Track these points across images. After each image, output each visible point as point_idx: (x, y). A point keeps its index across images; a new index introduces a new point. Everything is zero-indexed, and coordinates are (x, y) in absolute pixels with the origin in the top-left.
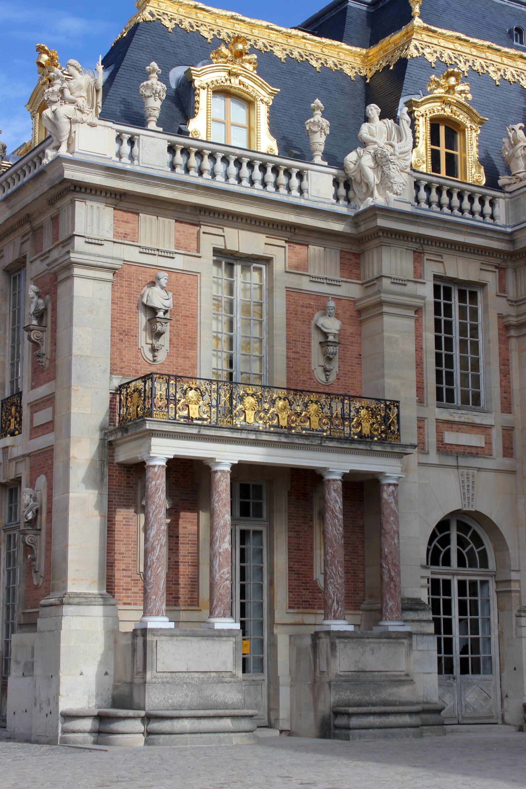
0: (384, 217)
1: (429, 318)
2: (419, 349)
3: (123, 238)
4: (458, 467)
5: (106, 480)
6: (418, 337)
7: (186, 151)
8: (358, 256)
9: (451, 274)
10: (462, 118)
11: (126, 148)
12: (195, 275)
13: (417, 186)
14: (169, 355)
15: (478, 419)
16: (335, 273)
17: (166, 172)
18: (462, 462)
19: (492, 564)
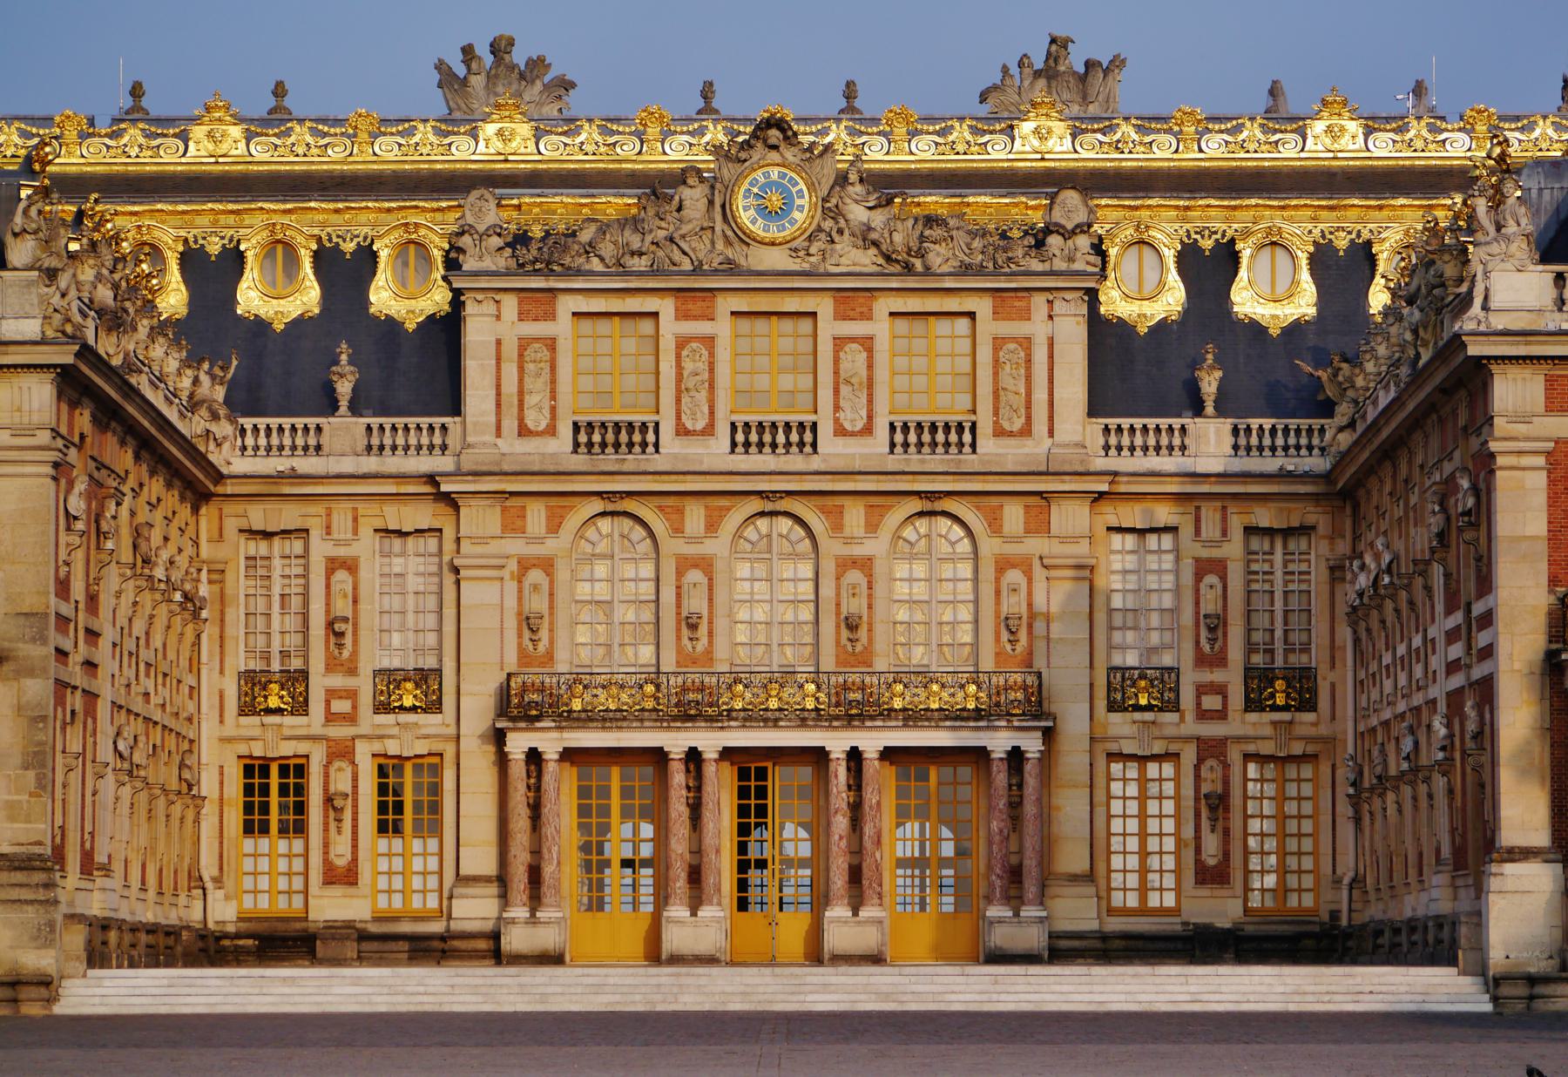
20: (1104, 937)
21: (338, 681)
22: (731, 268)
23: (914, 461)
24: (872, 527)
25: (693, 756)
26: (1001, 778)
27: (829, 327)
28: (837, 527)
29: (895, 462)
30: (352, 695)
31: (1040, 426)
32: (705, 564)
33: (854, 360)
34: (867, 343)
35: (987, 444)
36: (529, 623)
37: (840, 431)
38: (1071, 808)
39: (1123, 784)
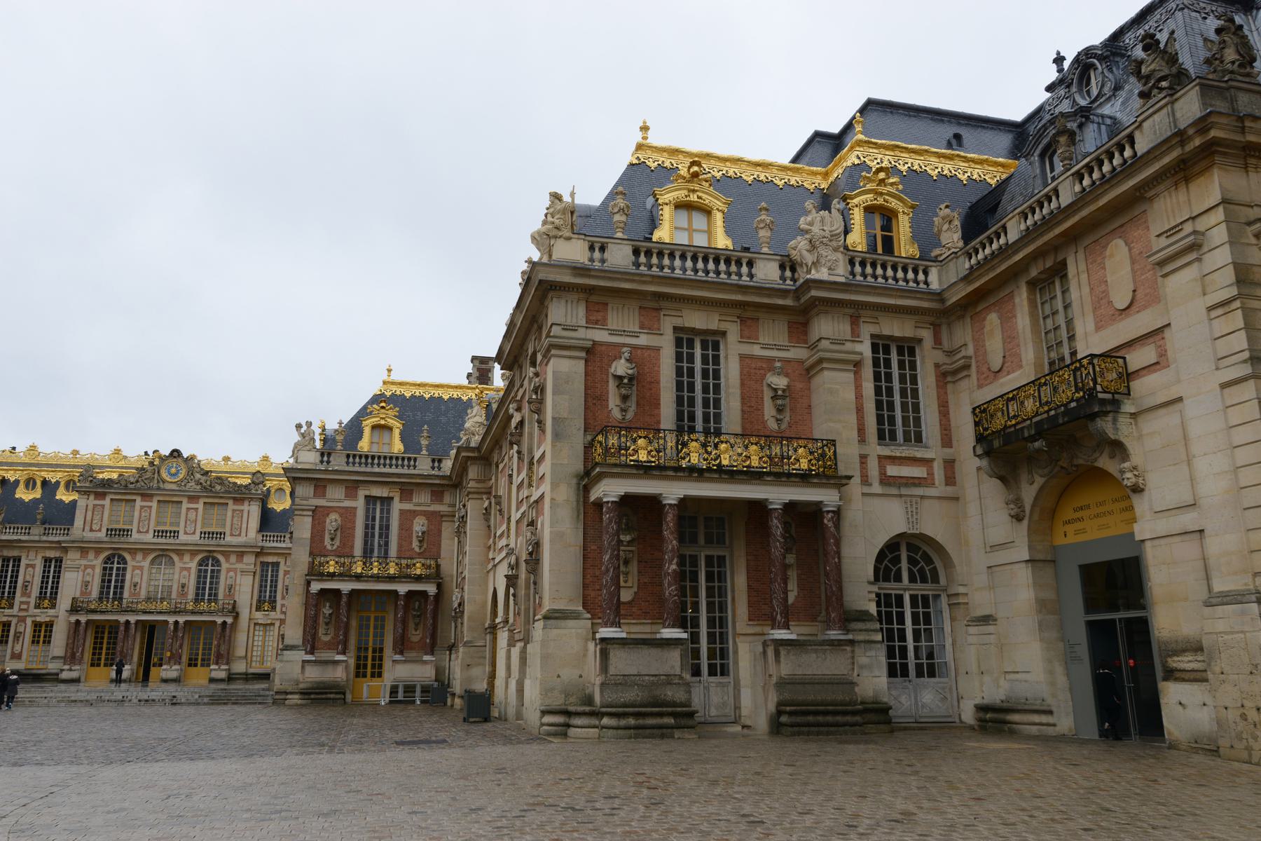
0: (818, 288)
1: (868, 372)
2: (859, 396)
3: (592, 323)
4: (901, 496)
5: (582, 517)
6: (858, 387)
7: (649, 253)
8: (806, 324)
9: (886, 332)
10: (894, 204)
11: (597, 254)
12: (657, 349)
13: (852, 262)
14: (636, 414)
15: (919, 453)
16: (783, 339)
17: (632, 269)
18: (904, 491)
19: (943, 581)
20: (246, 674)
21: (24, 599)
22: (159, 488)
23: (206, 542)
24: (192, 559)
25: (128, 622)
26: (219, 629)
27: (185, 505)
28: (181, 559)
29: (202, 542)
30: (28, 603)
31: (243, 534)
32: (141, 568)
33: (192, 515)
34: (196, 509)
35: (228, 538)
36: (86, 584)
37: (186, 533)
38: (241, 638)
39: (259, 633)
